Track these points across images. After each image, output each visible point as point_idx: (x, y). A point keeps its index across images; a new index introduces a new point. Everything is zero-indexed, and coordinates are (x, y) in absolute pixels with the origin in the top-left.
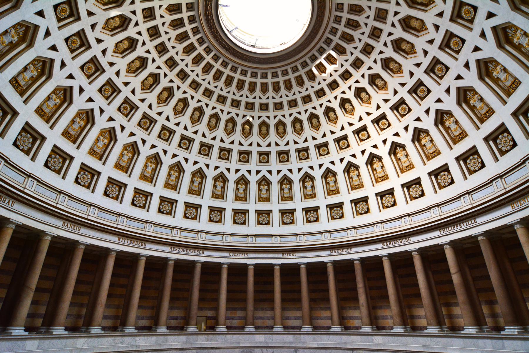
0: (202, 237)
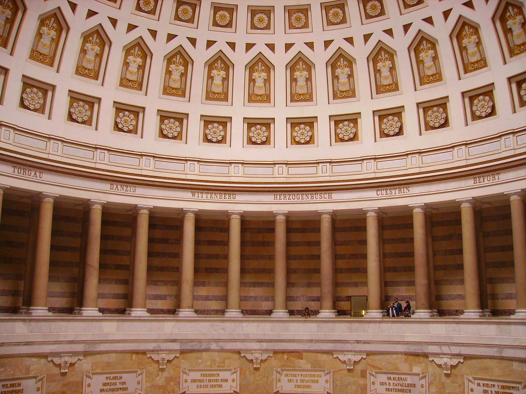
0: (324, 171)
